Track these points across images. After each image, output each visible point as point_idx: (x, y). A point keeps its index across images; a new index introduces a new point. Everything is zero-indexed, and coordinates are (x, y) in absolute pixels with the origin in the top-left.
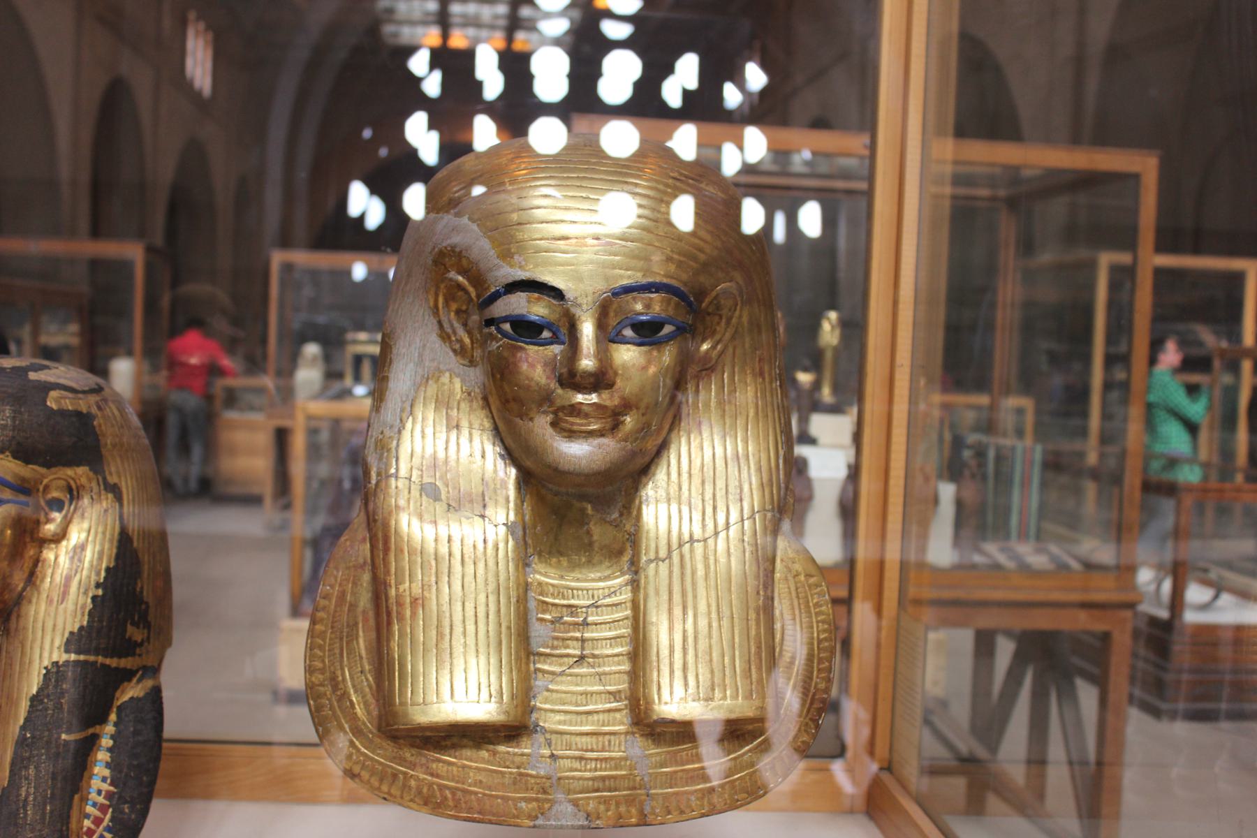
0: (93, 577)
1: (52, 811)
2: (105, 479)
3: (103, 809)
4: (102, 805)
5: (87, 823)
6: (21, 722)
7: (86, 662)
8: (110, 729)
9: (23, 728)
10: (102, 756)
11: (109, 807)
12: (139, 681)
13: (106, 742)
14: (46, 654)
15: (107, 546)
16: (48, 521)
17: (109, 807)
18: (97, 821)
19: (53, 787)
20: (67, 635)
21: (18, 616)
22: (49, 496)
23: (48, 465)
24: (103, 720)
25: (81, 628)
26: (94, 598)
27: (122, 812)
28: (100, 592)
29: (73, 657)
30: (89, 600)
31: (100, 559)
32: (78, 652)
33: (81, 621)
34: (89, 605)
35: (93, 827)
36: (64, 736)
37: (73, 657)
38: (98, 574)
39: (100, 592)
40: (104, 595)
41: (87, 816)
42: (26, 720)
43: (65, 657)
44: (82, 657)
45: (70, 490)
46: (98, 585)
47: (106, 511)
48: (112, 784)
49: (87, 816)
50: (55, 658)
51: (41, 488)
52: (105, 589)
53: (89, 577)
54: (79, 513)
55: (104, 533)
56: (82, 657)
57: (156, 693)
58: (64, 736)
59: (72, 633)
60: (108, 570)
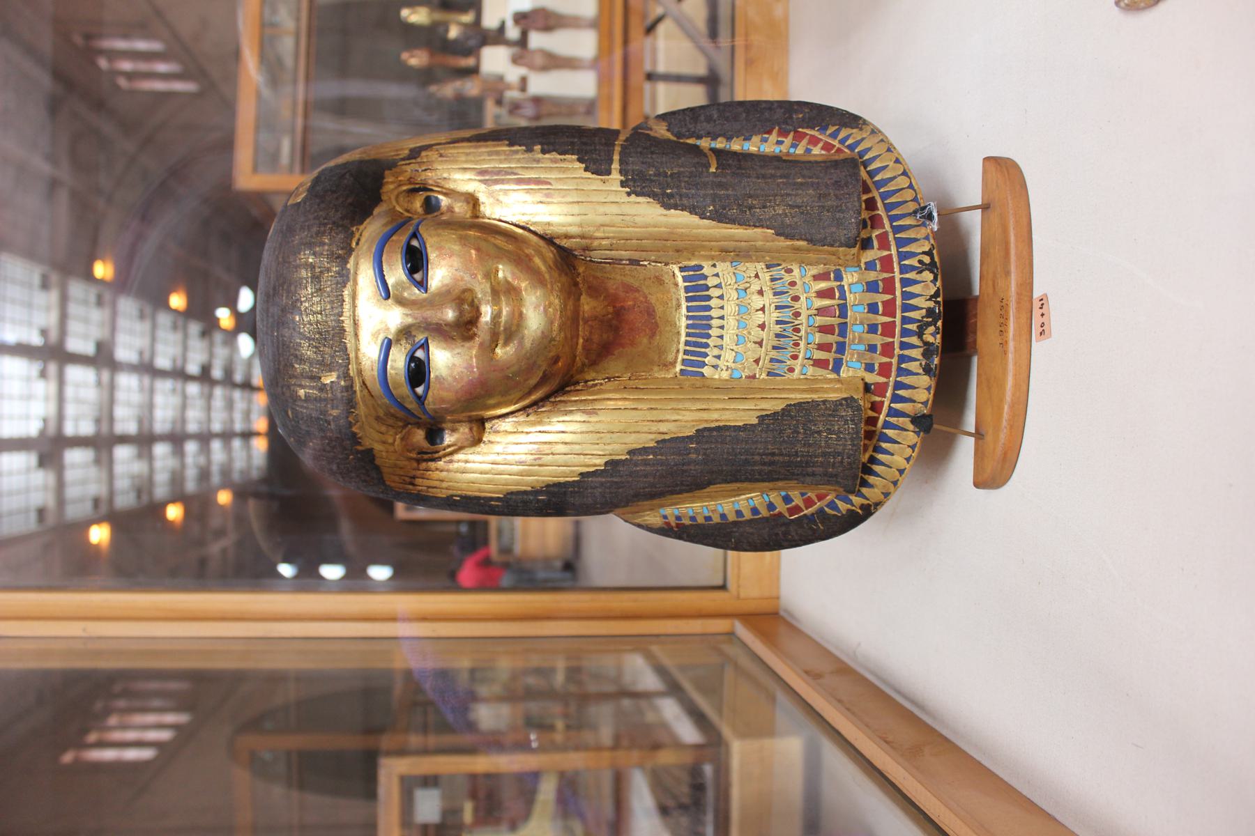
0: (520, 156)
1: (804, 177)
2: (403, 159)
3: (799, 137)
4: (794, 139)
5: (817, 151)
6: (695, 219)
7: (621, 162)
8: (705, 143)
9: (703, 217)
10: (736, 146)
11: (796, 132)
12: (651, 129)
13: (720, 144)
14: (612, 198)
15: (484, 150)
16: (450, 209)
17: (796, 132)
18: (814, 141)
19: (773, 176)
20: (588, 175)
21: (567, 236)
22: (420, 210)
23: (377, 199)
24: (696, 150)
25: (580, 160)
26: (544, 152)
27: (803, 119)
28: (538, 148)
29: (615, 166)
30: (547, 156)
31: (497, 153)
32: (611, 161)
33: (571, 161)
34: (555, 155)
35: (820, 145)
36: (713, 170)
37: (615, 166)
38: (516, 152)
39: (538, 148)
40: (541, 144)
41: (808, 151)
42: (692, 210)
43: (616, 176)
44: (616, 157)
45: (414, 191)
46: (530, 150)
47: (441, 156)
48: (769, 132)
49: (808, 151)
50: (616, 187)
51: (407, 214)
52: (535, 144)
53: (519, 161)
54: (443, 183)
55: (467, 154)
56: (616, 157)
57: (663, 117)
58: (713, 170)
59: (586, 170)
60: (511, 145)
